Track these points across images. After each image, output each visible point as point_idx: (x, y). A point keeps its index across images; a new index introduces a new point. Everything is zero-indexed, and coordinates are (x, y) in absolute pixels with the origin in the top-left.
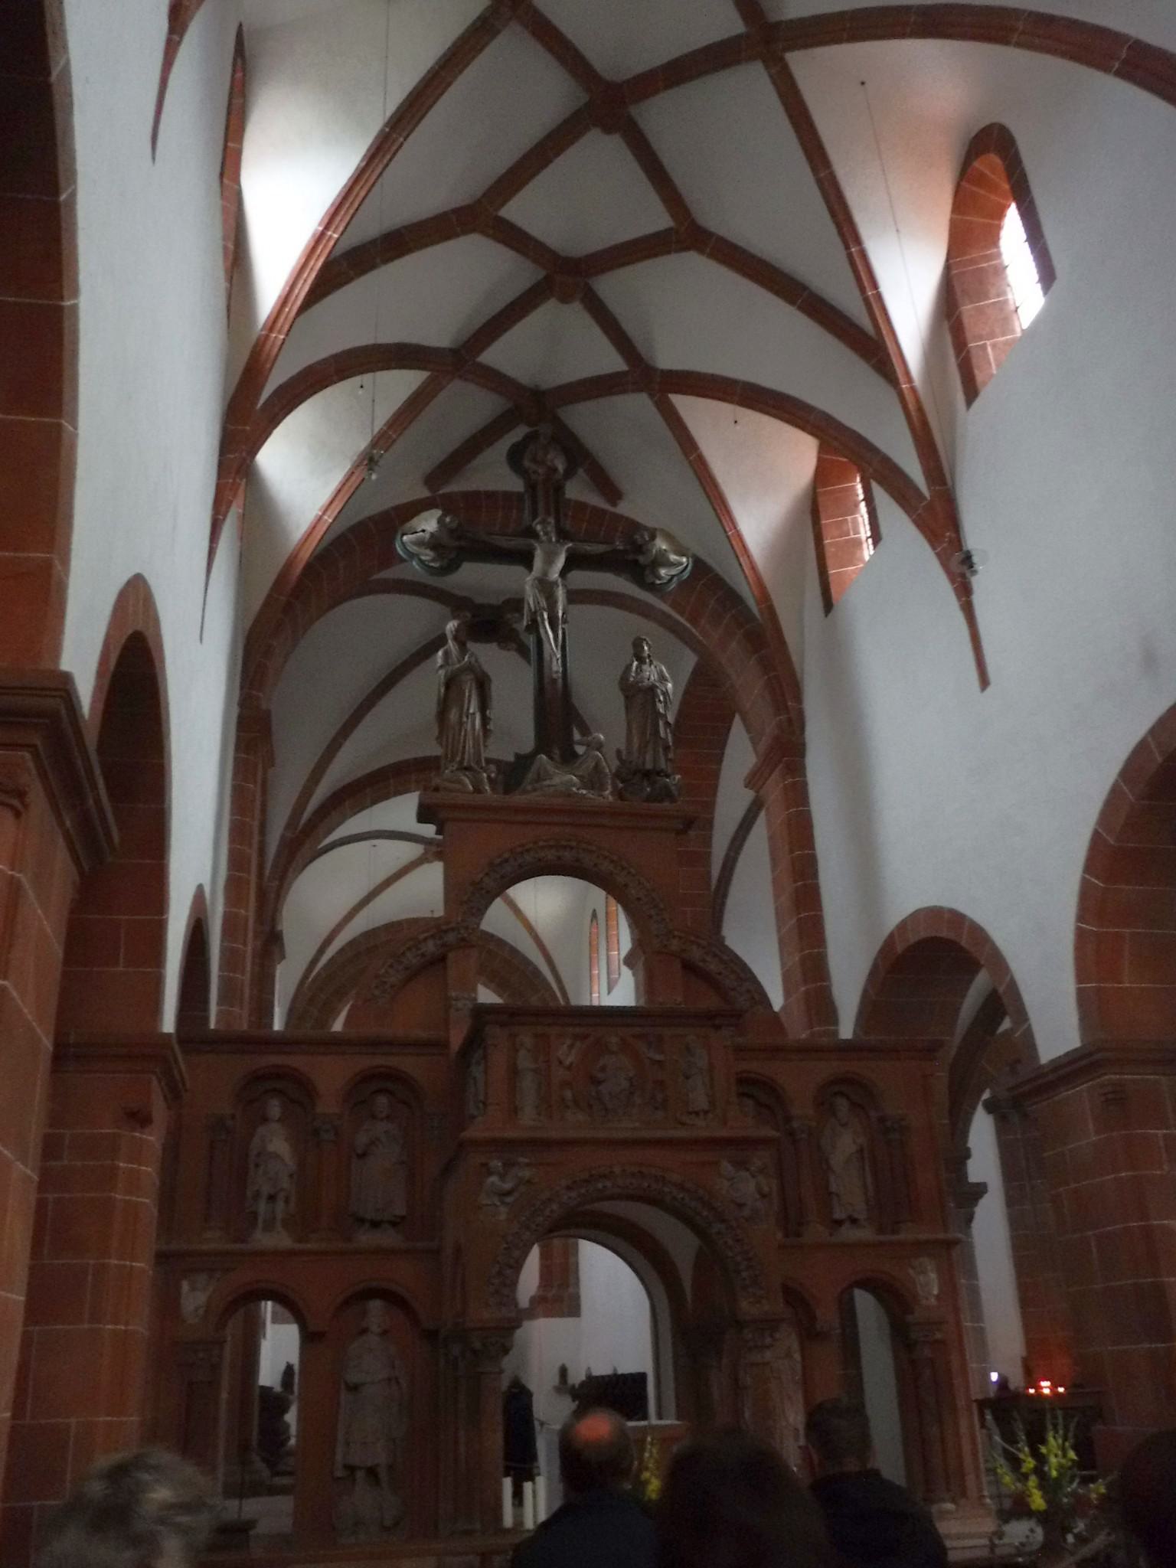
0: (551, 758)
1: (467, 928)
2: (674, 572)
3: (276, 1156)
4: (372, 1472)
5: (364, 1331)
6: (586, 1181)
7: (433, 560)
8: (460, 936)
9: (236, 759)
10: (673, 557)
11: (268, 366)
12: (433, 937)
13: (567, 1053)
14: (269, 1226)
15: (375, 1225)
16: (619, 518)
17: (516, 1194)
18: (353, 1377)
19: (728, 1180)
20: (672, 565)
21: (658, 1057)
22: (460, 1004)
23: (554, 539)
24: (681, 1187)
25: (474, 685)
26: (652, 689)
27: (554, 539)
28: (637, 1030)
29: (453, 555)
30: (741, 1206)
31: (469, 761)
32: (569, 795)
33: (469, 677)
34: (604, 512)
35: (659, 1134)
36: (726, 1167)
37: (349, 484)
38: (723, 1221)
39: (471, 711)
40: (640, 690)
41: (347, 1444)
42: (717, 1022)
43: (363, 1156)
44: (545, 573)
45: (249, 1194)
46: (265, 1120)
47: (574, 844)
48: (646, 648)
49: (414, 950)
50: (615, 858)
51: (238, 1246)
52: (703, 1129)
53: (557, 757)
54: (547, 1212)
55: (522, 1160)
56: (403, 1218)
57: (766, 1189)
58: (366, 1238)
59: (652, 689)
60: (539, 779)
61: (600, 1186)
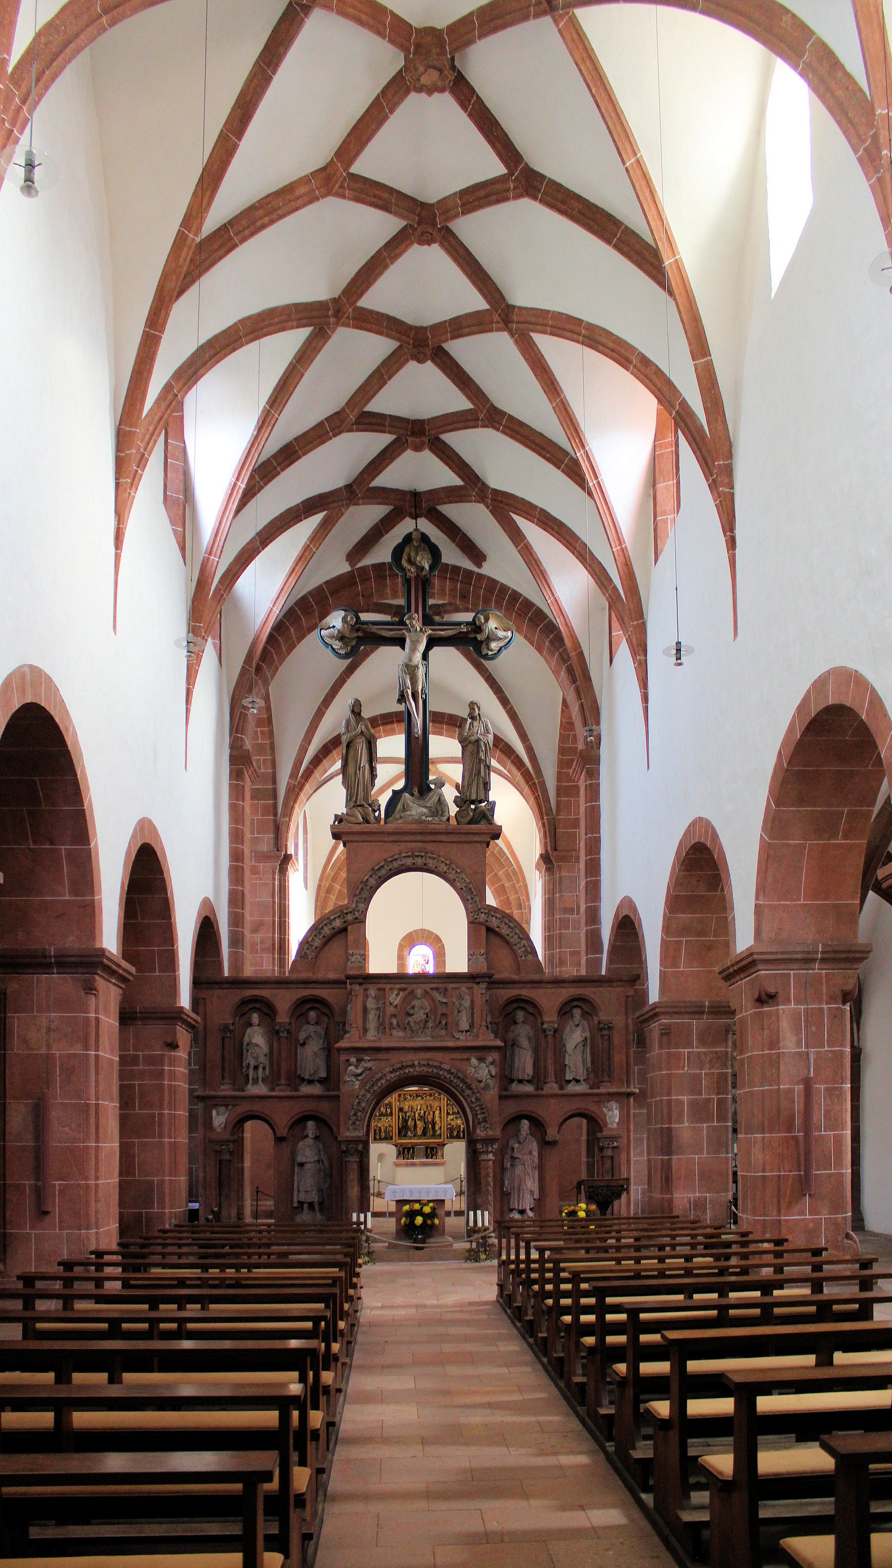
3: (257, 1045)
4: (311, 1205)
5: (307, 1136)
6: (401, 1069)
9: (230, 784)
12: (339, 917)
13: (395, 998)
14: (255, 1081)
15: (310, 1082)
18: (300, 1159)
23: (418, 629)
24: (449, 1072)
27: (418, 629)
29: (354, 643)
30: (480, 1081)
32: (421, 822)
35: (437, 1044)
36: (474, 1061)
37: (288, 584)
38: (471, 1089)
41: (299, 1191)
42: (477, 980)
43: (304, 1044)
44: (410, 660)
46: (251, 1025)
51: (237, 1093)
52: (464, 1040)
56: (325, 1079)
57: (494, 1073)
58: (306, 1089)
60: (404, 809)
61: (407, 1071)
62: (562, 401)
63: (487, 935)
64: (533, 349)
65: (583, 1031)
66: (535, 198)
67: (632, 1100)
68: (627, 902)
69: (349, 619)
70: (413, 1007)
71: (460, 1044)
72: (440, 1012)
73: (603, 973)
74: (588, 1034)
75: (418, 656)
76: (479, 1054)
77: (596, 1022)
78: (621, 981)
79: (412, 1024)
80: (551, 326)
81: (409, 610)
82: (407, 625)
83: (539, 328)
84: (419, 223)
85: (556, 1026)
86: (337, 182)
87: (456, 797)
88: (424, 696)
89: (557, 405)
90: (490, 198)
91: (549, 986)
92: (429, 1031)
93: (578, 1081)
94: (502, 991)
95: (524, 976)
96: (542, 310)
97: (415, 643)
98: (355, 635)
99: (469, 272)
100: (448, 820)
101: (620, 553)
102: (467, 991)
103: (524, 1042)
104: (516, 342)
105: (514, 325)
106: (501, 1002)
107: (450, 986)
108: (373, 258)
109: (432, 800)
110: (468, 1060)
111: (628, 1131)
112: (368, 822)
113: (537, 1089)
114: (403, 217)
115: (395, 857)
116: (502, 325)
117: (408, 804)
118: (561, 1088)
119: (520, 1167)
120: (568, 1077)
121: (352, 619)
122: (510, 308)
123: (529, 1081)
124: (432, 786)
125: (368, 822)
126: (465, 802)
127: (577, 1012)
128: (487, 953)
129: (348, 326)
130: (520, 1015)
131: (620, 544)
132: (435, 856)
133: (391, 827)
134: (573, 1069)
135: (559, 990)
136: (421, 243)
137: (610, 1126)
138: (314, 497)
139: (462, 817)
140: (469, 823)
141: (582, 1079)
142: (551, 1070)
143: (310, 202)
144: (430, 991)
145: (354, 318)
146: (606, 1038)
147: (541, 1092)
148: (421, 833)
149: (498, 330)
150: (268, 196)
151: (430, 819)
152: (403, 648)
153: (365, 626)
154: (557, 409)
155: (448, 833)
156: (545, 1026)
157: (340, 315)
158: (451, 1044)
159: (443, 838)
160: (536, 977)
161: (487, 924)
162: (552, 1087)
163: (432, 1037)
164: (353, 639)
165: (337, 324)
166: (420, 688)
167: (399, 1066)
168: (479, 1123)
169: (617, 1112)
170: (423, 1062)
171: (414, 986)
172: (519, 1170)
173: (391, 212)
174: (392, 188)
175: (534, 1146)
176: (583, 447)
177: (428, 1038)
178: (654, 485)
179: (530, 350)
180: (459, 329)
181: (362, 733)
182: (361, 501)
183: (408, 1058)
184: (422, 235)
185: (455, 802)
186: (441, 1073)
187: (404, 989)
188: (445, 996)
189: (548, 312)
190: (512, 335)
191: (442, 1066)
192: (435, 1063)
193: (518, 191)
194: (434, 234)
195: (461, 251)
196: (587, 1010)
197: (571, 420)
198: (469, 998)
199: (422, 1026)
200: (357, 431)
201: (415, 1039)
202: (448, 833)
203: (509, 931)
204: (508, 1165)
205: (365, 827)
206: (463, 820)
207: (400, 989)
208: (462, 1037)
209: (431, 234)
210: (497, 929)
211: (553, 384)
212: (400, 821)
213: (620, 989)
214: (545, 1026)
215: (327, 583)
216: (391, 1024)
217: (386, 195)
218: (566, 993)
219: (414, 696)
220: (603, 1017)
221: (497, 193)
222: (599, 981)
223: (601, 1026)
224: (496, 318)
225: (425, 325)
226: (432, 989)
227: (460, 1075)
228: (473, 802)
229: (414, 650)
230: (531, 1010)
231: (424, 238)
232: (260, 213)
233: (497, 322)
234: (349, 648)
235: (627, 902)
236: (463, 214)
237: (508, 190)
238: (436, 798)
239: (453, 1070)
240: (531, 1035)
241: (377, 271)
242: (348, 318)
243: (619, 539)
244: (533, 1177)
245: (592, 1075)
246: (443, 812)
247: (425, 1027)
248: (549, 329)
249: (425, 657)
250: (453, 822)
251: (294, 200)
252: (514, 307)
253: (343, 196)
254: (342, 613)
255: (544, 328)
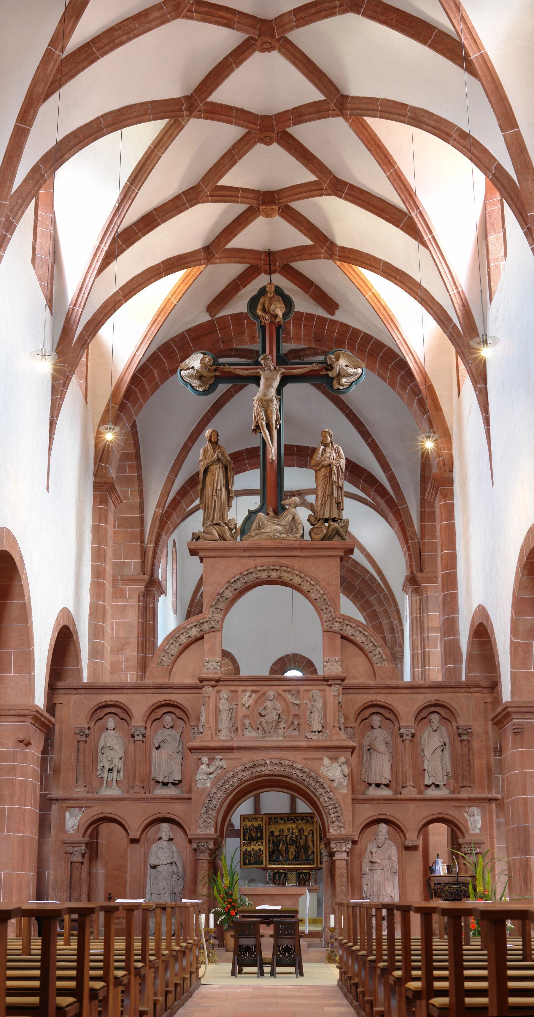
0: (268, 514)
1: (214, 620)
2: (352, 379)
7: (200, 386)
8: (210, 626)
10: (351, 370)
11: (74, 327)
16: (334, 322)
17: (215, 774)
19: (327, 768)
20: (350, 375)
21: (296, 702)
22: (209, 665)
23: (272, 368)
25: (221, 471)
26: (330, 465)
27: (272, 368)
28: (286, 688)
31: (217, 520)
33: (218, 466)
34: (325, 319)
36: (326, 761)
39: (219, 488)
40: (323, 466)
45: (99, 768)
47: (277, 568)
48: (329, 438)
49: (185, 634)
50: (302, 575)
53: (271, 513)
54: (231, 783)
55: (217, 757)
59: (330, 465)
60: (259, 528)
62: (395, 170)
63: (342, 643)
64: (366, 130)
65: (441, 736)
66: (358, 12)
67: (494, 806)
68: (482, 611)
69: (207, 360)
70: (265, 708)
71: (312, 744)
72: (292, 714)
73: (463, 679)
74: (447, 741)
75: (273, 391)
76: (332, 754)
77: (455, 728)
78: (478, 686)
79: (265, 725)
80: (380, 111)
81: (264, 351)
82: (261, 365)
83: (370, 113)
84: (259, 36)
85: (413, 731)
86: (185, 7)
87: (310, 516)
88: (278, 427)
89: (391, 173)
90: (320, 14)
91: (405, 691)
92: (281, 732)
93: (437, 786)
94: (358, 697)
95: (379, 682)
96: (372, 98)
97: (269, 381)
98: (213, 374)
99: (306, 72)
100: (302, 536)
101: (457, 296)
102: (319, 693)
103: (381, 747)
104: (351, 125)
105: (348, 112)
106: (356, 707)
107: (302, 688)
108: (220, 63)
109: (286, 518)
110: (321, 759)
111: (492, 837)
112: (224, 539)
113: (396, 793)
114: (245, 31)
115: (252, 570)
116: (337, 112)
117: (263, 523)
118: (421, 793)
119: (379, 872)
120: (428, 782)
121: (210, 361)
122: (344, 98)
123: (387, 786)
124: (287, 507)
125: (224, 539)
126: (319, 520)
127: (435, 718)
128: (342, 661)
129: (200, 117)
130: (376, 720)
131: (457, 288)
132: (289, 570)
133: (246, 543)
134: (432, 773)
135: (415, 696)
136: (262, 50)
137: (472, 832)
138: (174, 257)
139: (316, 534)
140: (322, 540)
141: (441, 784)
142: (410, 776)
143: (163, 23)
144: (282, 693)
145: (206, 111)
146: (465, 743)
147: (399, 796)
148: (276, 549)
149: (334, 116)
150: (126, 20)
151: (285, 536)
152: (258, 385)
153: (222, 367)
154: (391, 177)
155: (302, 549)
156: (402, 731)
157: (193, 108)
158: (303, 744)
159: (298, 553)
160: (393, 683)
161: (342, 632)
162: (410, 792)
163: (285, 737)
164: (212, 377)
165: (190, 116)
166: (274, 419)
167: (251, 764)
168: (333, 822)
169: (478, 818)
170: (274, 761)
171: (268, 688)
172: (378, 875)
173: (234, 29)
174: (235, 10)
175: (393, 851)
176: (418, 208)
177: (280, 738)
178: (486, 237)
179: (364, 131)
180: (300, 116)
181: (219, 460)
182: (218, 261)
183: (259, 757)
184: (262, 45)
185: (309, 520)
186: (293, 772)
187: (258, 691)
188: (298, 698)
189: (378, 99)
190: (347, 120)
191: (295, 765)
192: (287, 763)
193: (343, 7)
194: (273, 43)
195: (298, 56)
196: (445, 715)
197: (405, 186)
198: (321, 700)
199: (274, 725)
200: (212, 201)
201: (267, 739)
202: (302, 549)
203: (364, 639)
204: (367, 870)
205: (222, 544)
206: (317, 537)
207: (253, 692)
208: (315, 737)
209: (270, 44)
210: (352, 637)
211: (386, 157)
212: (255, 538)
213: (479, 695)
214: (402, 731)
215: (188, 331)
216: (244, 724)
217: (229, 16)
218: (422, 699)
219: (269, 426)
220: (462, 722)
221: (325, 10)
222: (457, 687)
223: (460, 731)
224: (332, 106)
225: (270, 115)
226: (284, 691)
227: (313, 774)
228: (326, 520)
229: (268, 386)
230: (388, 715)
231: (265, 46)
232: (119, 33)
233: (333, 110)
234: (207, 386)
235: (482, 611)
236: (297, 27)
237: (335, 7)
238: (290, 517)
239: (305, 770)
240: (389, 739)
241: (225, 74)
242: (200, 111)
243: (455, 283)
244: (393, 883)
245: (452, 781)
246: (297, 530)
247: (277, 728)
248: (378, 113)
249: (279, 392)
250: (307, 537)
251: (148, 23)
252: (347, 97)
253: (191, 18)
254: (202, 356)
255: (374, 112)
